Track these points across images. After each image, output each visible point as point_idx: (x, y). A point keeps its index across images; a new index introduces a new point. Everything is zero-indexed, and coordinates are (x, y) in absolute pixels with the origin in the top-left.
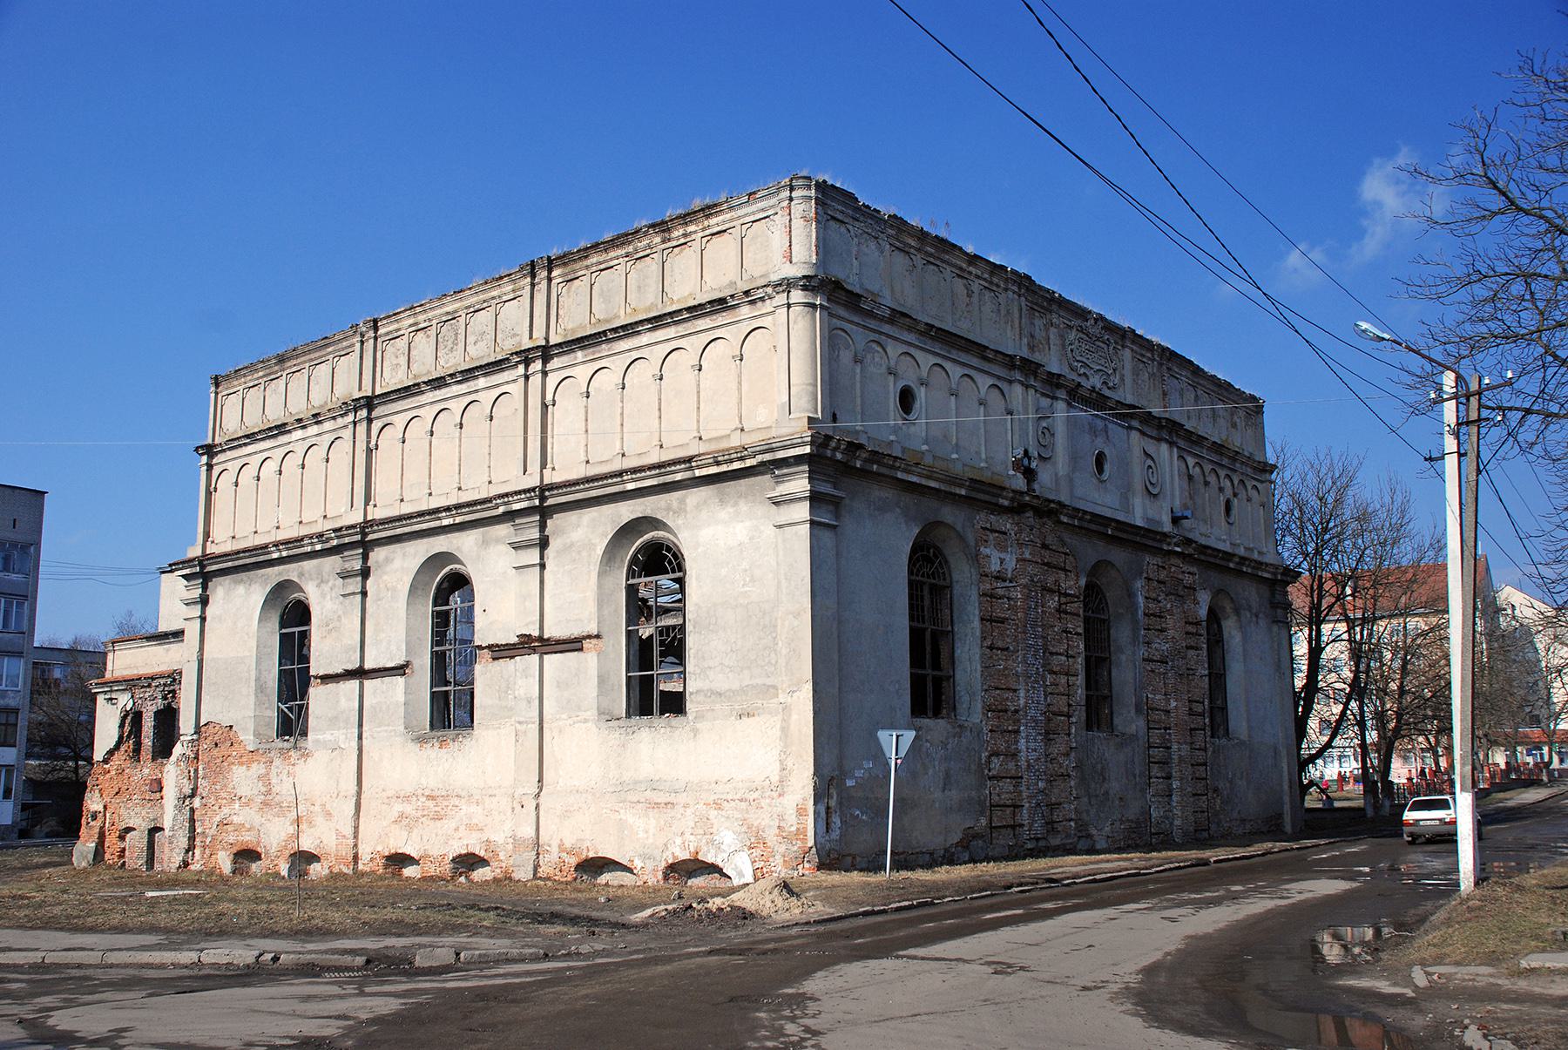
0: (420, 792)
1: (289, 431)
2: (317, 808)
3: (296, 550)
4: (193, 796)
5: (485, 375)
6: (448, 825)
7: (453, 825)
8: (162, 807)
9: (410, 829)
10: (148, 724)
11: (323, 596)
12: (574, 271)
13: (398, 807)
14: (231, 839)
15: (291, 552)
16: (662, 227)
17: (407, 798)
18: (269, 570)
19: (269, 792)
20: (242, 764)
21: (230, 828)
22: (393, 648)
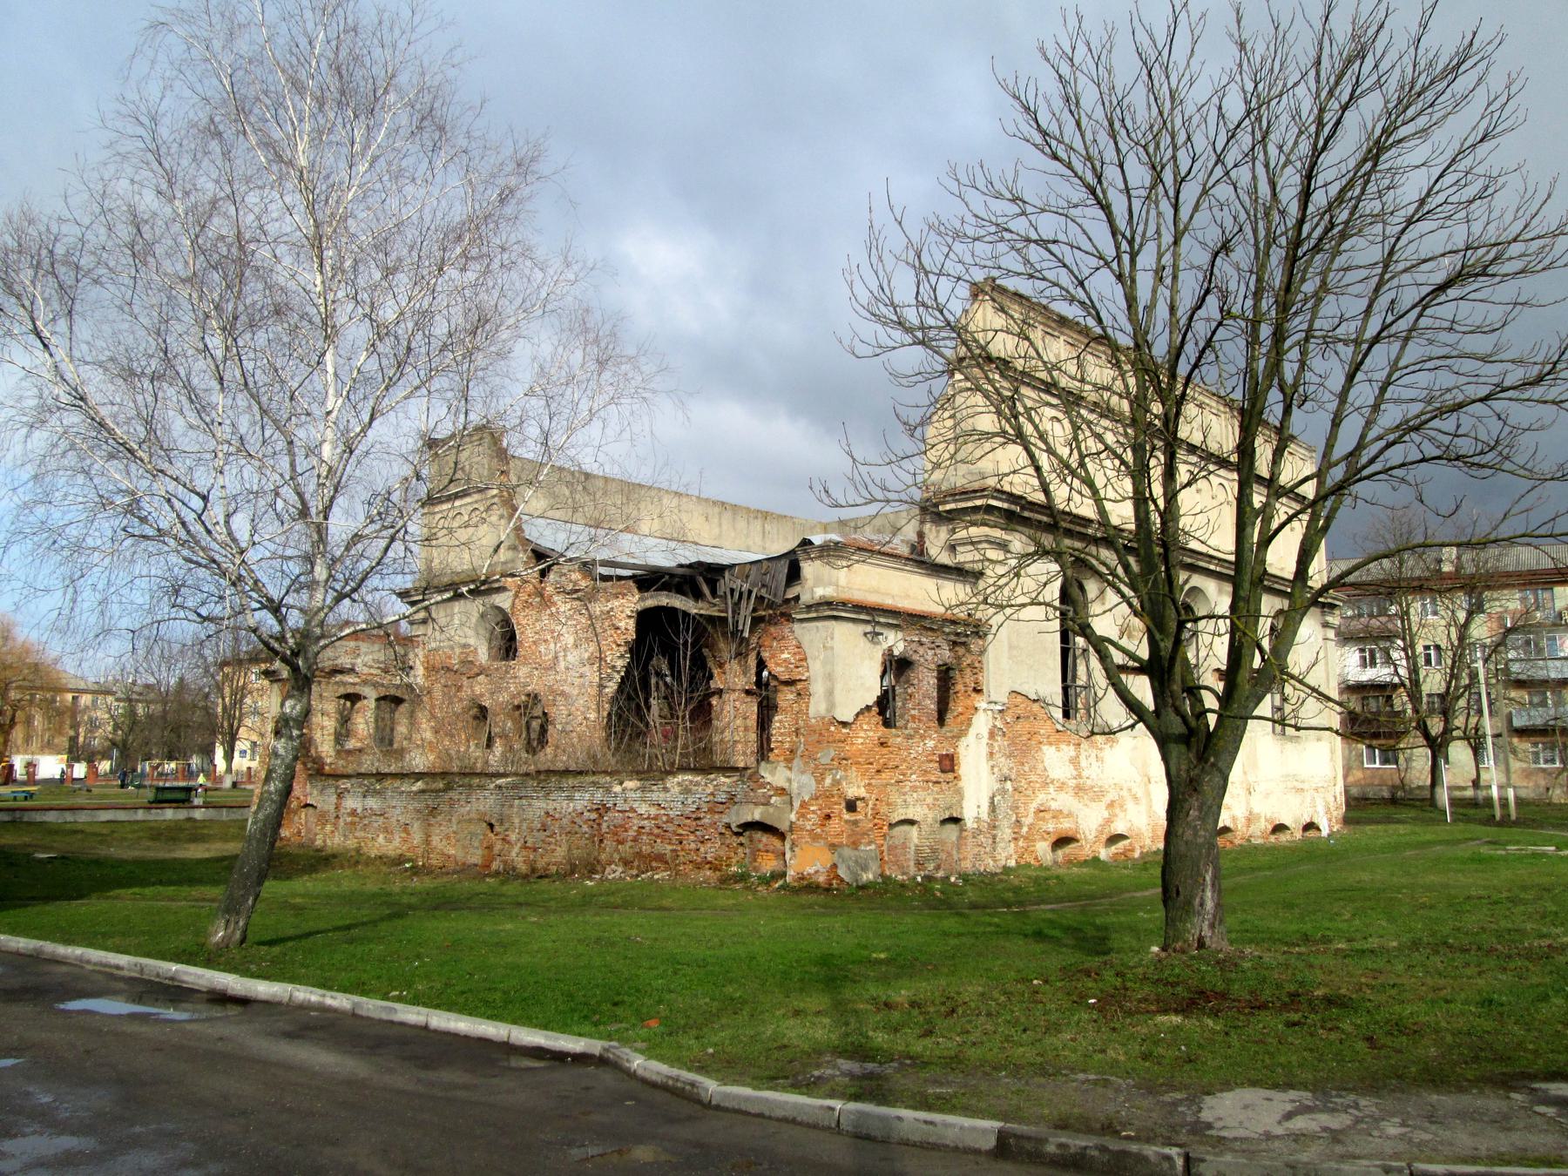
8: (959, 793)
10: (926, 681)
14: (1051, 827)
19: (1080, 776)
21: (1048, 815)
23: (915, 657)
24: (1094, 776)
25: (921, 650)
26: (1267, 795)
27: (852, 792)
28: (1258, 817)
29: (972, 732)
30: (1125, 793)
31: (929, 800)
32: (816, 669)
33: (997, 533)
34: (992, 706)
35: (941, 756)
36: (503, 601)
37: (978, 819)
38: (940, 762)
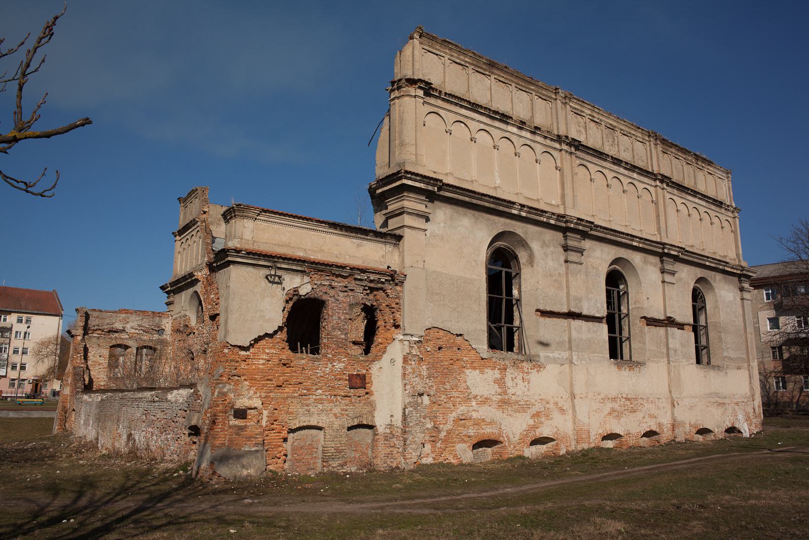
0: (620, 396)
1: (507, 123)
2: (551, 406)
3: (534, 217)
4: (421, 395)
5: (639, 174)
6: (639, 415)
7: (642, 415)
9: (618, 417)
11: (546, 255)
12: (667, 150)
13: (609, 405)
14: (471, 432)
15: (530, 216)
16: (697, 157)
17: (614, 399)
18: (502, 220)
19: (505, 393)
20: (474, 368)
21: (468, 423)
22: (599, 305)
23: (325, 297)
24: (519, 393)
25: (332, 292)
26: (691, 408)
27: (241, 403)
28: (683, 424)
29: (386, 358)
30: (551, 406)
31: (337, 410)
32: (222, 302)
33: (421, 207)
34: (409, 338)
35: (349, 375)
36: (199, 288)
37: (391, 426)
38: (350, 380)
